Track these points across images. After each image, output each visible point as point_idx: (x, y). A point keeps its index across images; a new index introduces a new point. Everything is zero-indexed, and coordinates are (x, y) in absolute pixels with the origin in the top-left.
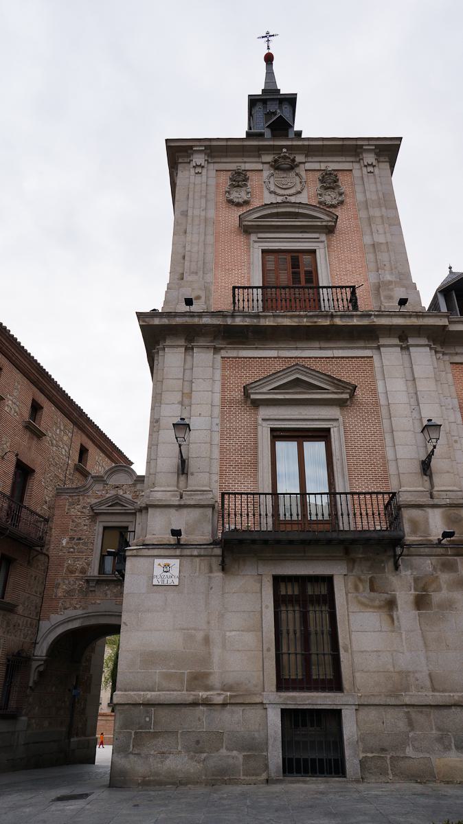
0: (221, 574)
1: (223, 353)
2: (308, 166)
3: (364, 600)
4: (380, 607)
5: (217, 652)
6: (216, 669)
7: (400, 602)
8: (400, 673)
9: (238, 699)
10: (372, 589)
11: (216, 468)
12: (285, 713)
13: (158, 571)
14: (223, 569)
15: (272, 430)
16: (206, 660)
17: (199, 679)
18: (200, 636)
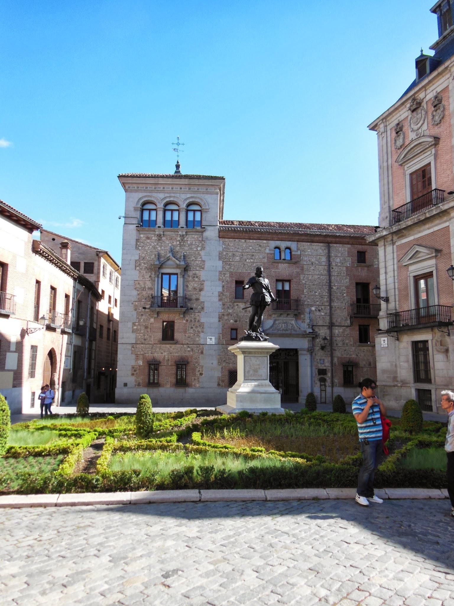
0: (397, 342)
1: (397, 244)
2: (428, 98)
3: (439, 350)
4: (443, 352)
5: (398, 369)
6: (399, 375)
7: (450, 349)
8: (449, 377)
9: (404, 383)
10: (441, 345)
11: (397, 300)
12: (416, 389)
13: (382, 342)
14: (398, 340)
15: (415, 277)
16: (396, 372)
17: (395, 378)
18: (394, 364)
